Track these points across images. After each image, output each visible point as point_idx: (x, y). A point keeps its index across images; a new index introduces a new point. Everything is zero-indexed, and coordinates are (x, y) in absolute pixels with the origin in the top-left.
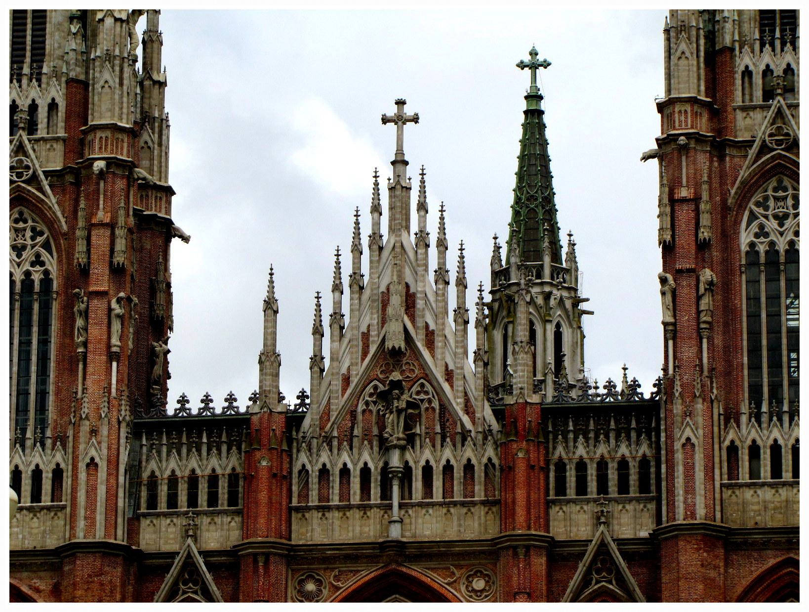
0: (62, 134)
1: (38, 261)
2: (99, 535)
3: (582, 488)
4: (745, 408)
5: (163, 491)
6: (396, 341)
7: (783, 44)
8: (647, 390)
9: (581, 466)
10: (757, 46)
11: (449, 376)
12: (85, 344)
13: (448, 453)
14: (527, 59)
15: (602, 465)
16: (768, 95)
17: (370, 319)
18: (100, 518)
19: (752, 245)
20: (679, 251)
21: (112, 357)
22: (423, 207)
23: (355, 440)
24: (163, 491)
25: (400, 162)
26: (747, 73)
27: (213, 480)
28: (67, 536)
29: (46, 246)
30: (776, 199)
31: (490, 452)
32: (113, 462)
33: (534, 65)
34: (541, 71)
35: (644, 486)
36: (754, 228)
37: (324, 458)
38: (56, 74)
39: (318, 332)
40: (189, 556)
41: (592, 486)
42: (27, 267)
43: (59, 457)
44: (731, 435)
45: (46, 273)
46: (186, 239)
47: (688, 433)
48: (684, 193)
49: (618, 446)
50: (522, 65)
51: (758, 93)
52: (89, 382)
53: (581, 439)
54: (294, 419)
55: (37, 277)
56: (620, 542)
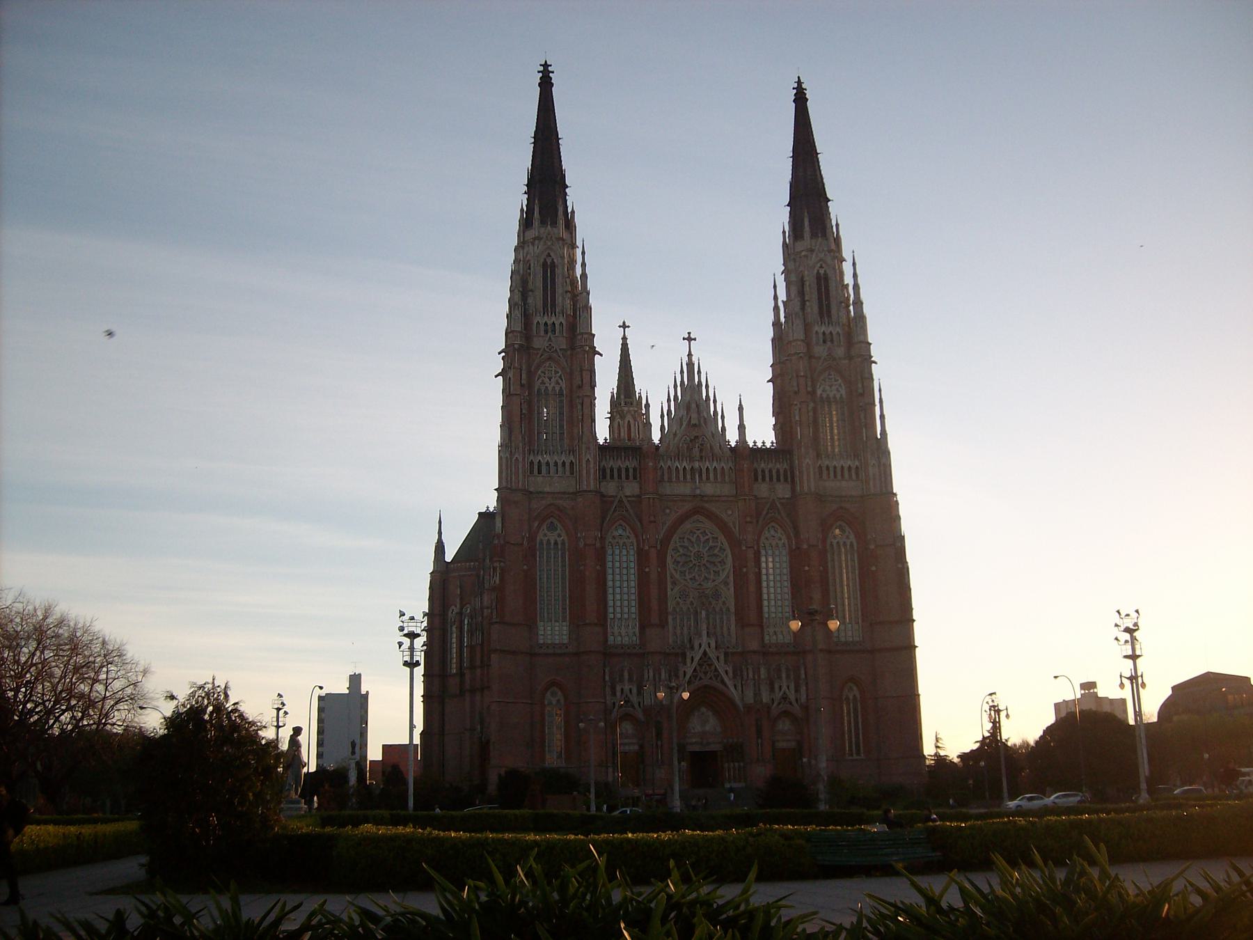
0: (565, 335)
2: (592, 487)
3: (764, 479)
5: (608, 471)
7: (829, 323)
9: (763, 471)
10: (820, 323)
11: (713, 435)
12: (583, 415)
13: (715, 464)
14: (622, 324)
15: (770, 471)
16: (824, 342)
17: (683, 412)
19: (821, 394)
22: (699, 372)
23: (680, 459)
24: (608, 471)
25: (690, 355)
26: (817, 332)
27: (627, 470)
28: (578, 487)
29: (560, 377)
30: (829, 379)
31: (730, 464)
33: (624, 326)
34: (627, 329)
35: (786, 480)
36: (821, 388)
37: (669, 463)
39: (662, 416)
40: (621, 497)
41: (767, 479)
42: (552, 385)
43: (572, 458)
45: (561, 388)
47: (807, 460)
48: (802, 374)
49: (775, 464)
50: (620, 327)
51: (821, 341)
52: (585, 429)
53: (763, 462)
55: (557, 389)
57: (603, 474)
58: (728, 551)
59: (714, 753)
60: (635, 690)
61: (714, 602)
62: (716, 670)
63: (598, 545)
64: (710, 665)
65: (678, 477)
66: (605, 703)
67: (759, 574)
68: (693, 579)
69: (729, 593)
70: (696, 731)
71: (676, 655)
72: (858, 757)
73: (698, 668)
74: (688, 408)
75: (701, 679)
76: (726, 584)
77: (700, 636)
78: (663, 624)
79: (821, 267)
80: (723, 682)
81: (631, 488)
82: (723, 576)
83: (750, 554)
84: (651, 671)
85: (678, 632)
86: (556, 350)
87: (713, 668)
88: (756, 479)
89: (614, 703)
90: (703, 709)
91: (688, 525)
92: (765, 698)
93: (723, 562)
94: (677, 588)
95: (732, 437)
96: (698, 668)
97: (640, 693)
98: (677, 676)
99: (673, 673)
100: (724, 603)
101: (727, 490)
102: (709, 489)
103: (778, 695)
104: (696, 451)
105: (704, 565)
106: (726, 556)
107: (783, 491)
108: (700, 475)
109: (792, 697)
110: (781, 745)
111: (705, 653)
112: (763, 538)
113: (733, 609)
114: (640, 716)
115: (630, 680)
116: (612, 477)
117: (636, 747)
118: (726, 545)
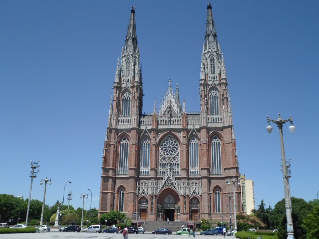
1: (129, 96)
4: (210, 114)
6: (169, 106)
12: (134, 105)
17: (167, 103)
18: (135, 125)
20: (202, 96)
21: (137, 107)
31: (180, 118)
32: (137, 119)
38: (131, 76)
44: (208, 117)
46: (144, 96)
57: (140, 123)
60: (146, 189)
61: (173, 161)
62: (172, 183)
64: (170, 181)
66: (136, 193)
68: (167, 155)
70: (167, 202)
72: (219, 213)
73: (166, 182)
75: (167, 185)
76: (178, 156)
79: (212, 56)
80: (174, 187)
82: (177, 153)
84: (151, 183)
85: (162, 171)
86: (128, 87)
87: (171, 182)
90: (169, 195)
93: (177, 149)
96: (166, 182)
97: (147, 190)
100: (177, 162)
101: (179, 127)
102: (173, 127)
103: (192, 191)
105: (171, 150)
106: (178, 147)
108: (171, 123)
109: (197, 191)
111: (169, 177)
118: (178, 144)
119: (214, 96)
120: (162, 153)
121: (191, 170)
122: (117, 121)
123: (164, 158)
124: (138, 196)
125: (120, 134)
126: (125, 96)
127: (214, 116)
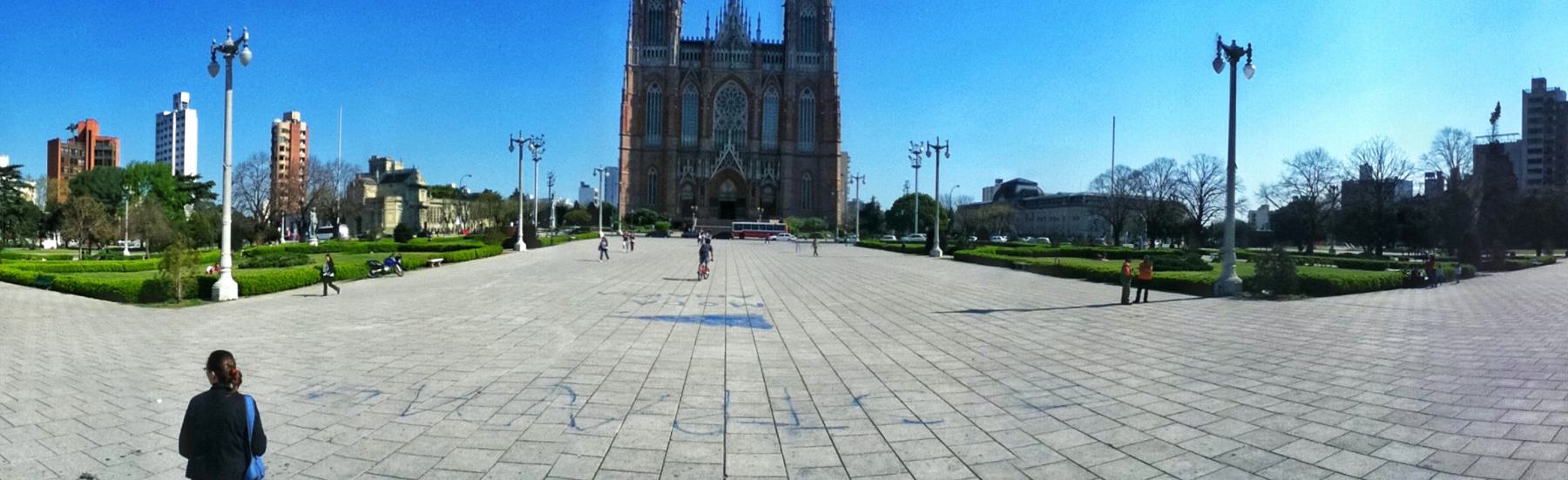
8: (780, 42)
9: (769, 57)
13: (743, 52)
17: (727, 22)
31: (751, 52)
39: (717, 25)
54: (712, 42)
56: (776, 72)
57: (682, 56)
58: (746, 100)
59: (733, 203)
63: (676, 95)
65: (722, 60)
67: (762, 112)
68: (727, 114)
69: (745, 122)
71: (714, 152)
74: (730, 20)
76: (744, 117)
77: (727, 142)
78: (709, 136)
81: (696, 64)
83: (756, 102)
88: (765, 61)
89: (681, 176)
90: (728, 181)
91: (726, 85)
92: (758, 176)
93: (743, 106)
94: (719, 118)
95: (754, 36)
97: (695, 171)
98: (714, 163)
99: (712, 162)
103: (765, 175)
104: (733, 45)
107: (778, 67)
109: (773, 177)
110: (764, 200)
111: (729, 153)
112: (765, 94)
113: (746, 130)
114: (695, 183)
115: (690, 165)
116: (687, 58)
117: (692, 198)
119: (808, 16)
120: (719, 112)
121: (765, 142)
122: (642, 53)
123: (722, 122)
124: (679, 180)
125: (646, 73)
126: (654, 4)
127: (807, 54)
